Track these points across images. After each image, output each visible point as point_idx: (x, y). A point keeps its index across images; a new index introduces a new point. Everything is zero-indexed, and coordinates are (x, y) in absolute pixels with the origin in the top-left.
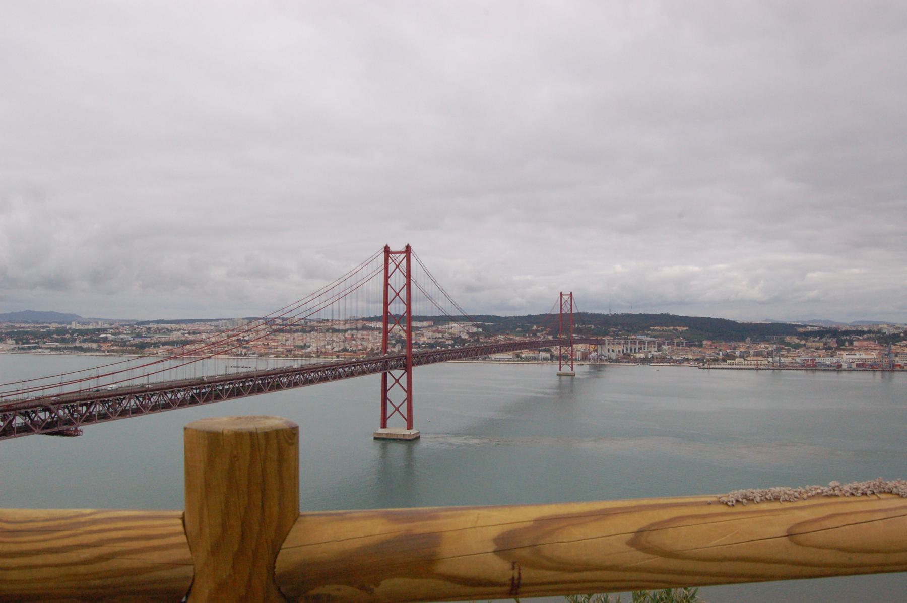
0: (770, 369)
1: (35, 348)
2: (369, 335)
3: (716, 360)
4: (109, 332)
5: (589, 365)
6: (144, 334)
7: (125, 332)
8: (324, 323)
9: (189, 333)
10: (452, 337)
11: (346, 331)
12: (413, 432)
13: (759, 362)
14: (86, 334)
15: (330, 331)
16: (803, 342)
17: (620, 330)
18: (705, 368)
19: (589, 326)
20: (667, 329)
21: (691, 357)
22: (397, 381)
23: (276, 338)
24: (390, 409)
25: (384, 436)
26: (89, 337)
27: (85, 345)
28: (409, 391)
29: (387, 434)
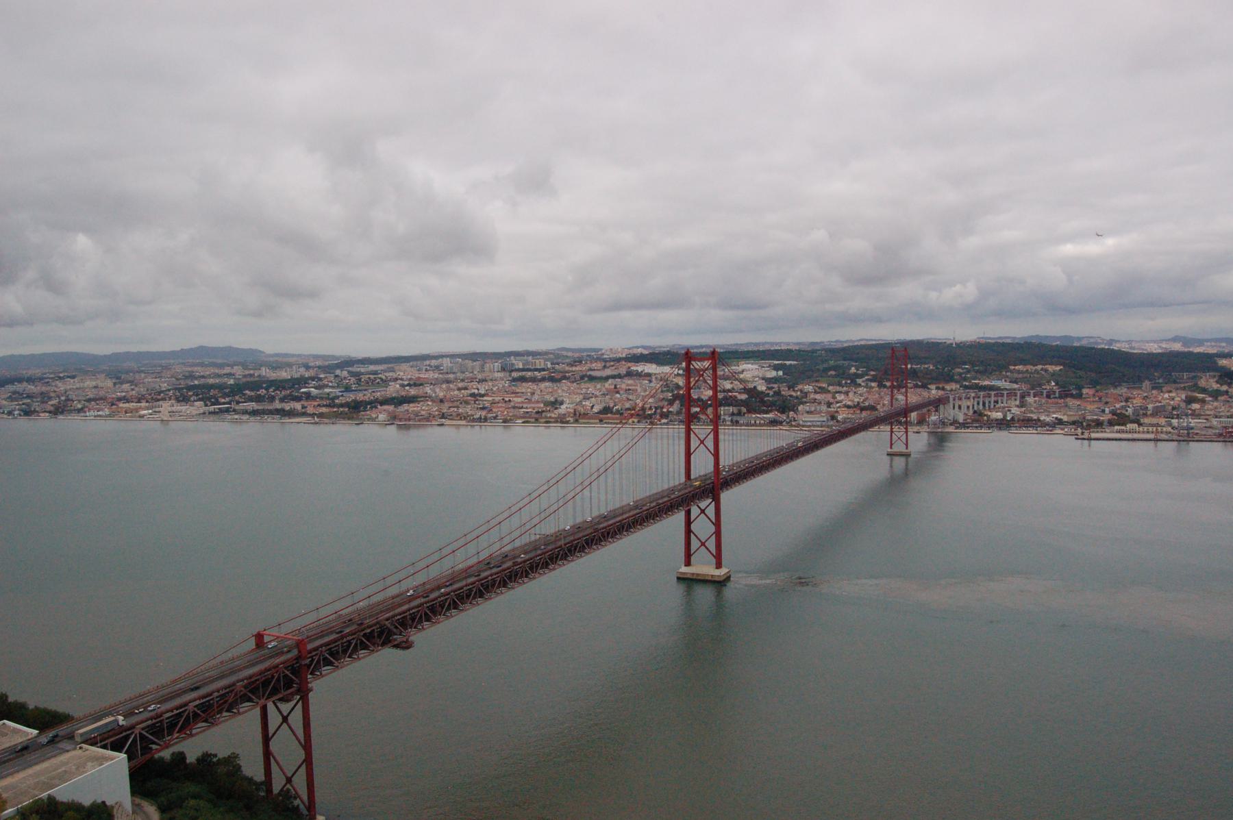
0: (1173, 441)
1: (227, 411)
2: (637, 386)
3: (1099, 424)
4: (311, 385)
5: (931, 432)
6: (354, 386)
7: (330, 384)
8: (576, 366)
9: (409, 385)
10: (745, 389)
11: (607, 378)
12: (722, 572)
13: (1159, 428)
14: (284, 388)
15: (586, 379)
16: (1225, 388)
17: (968, 371)
18: (1084, 439)
19: (926, 366)
20: (1034, 368)
21: (1065, 418)
22: (703, 511)
23: (518, 391)
24: (695, 544)
25: (689, 576)
26: (288, 392)
27: (287, 407)
28: (717, 524)
29: (693, 574)
